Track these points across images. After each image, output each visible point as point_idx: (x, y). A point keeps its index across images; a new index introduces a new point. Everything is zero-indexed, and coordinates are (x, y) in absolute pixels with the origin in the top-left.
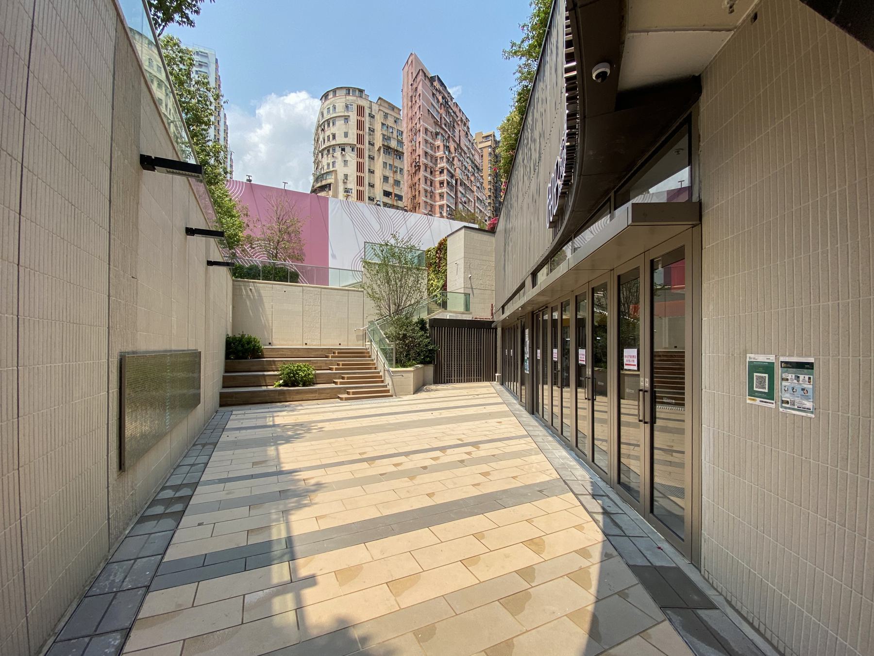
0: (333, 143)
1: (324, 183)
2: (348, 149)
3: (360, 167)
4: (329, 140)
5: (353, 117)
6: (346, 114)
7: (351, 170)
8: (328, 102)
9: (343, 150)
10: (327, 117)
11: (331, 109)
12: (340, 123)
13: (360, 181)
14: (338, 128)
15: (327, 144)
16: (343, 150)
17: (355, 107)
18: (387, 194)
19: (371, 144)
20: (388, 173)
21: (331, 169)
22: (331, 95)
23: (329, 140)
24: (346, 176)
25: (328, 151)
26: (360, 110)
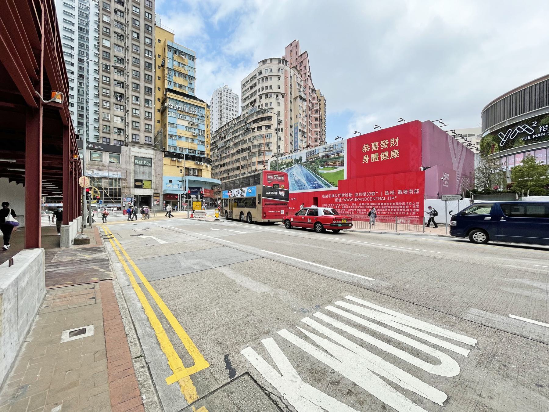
0: (270, 91)
1: (266, 115)
2: (280, 96)
3: (286, 107)
4: (267, 88)
5: (283, 75)
6: (279, 74)
7: (282, 109)
8: (265, 66)
9: (277, 96)
10: (264, 74)
11: (269, 70)
12: (275, 79)
14: (274, 82)
15: (265, 91)
16: (277, 96)
17: (283, 71)
19: (291, 94)
21: (269, 107)
22: (268, 62)
23: (267, 88)
24: (279, 112)
25: (267, 96)
26: (286, 72)
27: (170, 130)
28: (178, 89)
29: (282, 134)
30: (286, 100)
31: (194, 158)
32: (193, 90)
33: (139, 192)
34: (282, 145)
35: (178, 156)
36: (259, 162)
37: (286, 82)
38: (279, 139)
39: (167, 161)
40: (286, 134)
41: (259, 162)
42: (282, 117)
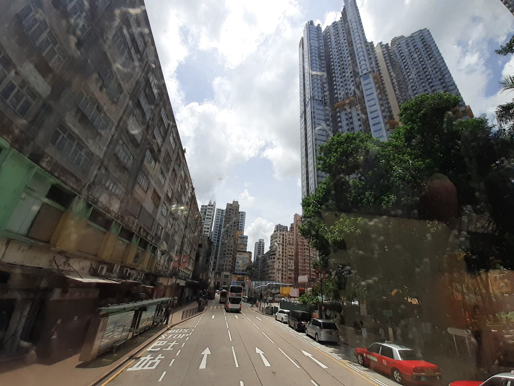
3: (283, 249)
5: (281, 236)
12: (278, 238)
13: (283, 252)
14: (278, 239)
18: (289, 255)
20: (290, 250)
26: (283, 235)
27: (236, 264)
28: (241, 250)
29: (280, 261)
30: (283, 245)
31: (242, 274)
32: (246, 249)
33: (224, 286)
34: (281, 265)
35: (237, 274)
36: (271, 273)
37: (283, 238)
38: (279, 262)
39: (233, 275)
40: (283, 260)
41: (271, 273)
42: (281, 253)
